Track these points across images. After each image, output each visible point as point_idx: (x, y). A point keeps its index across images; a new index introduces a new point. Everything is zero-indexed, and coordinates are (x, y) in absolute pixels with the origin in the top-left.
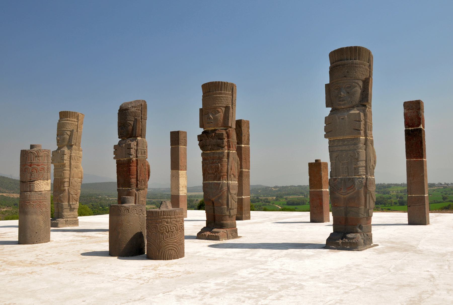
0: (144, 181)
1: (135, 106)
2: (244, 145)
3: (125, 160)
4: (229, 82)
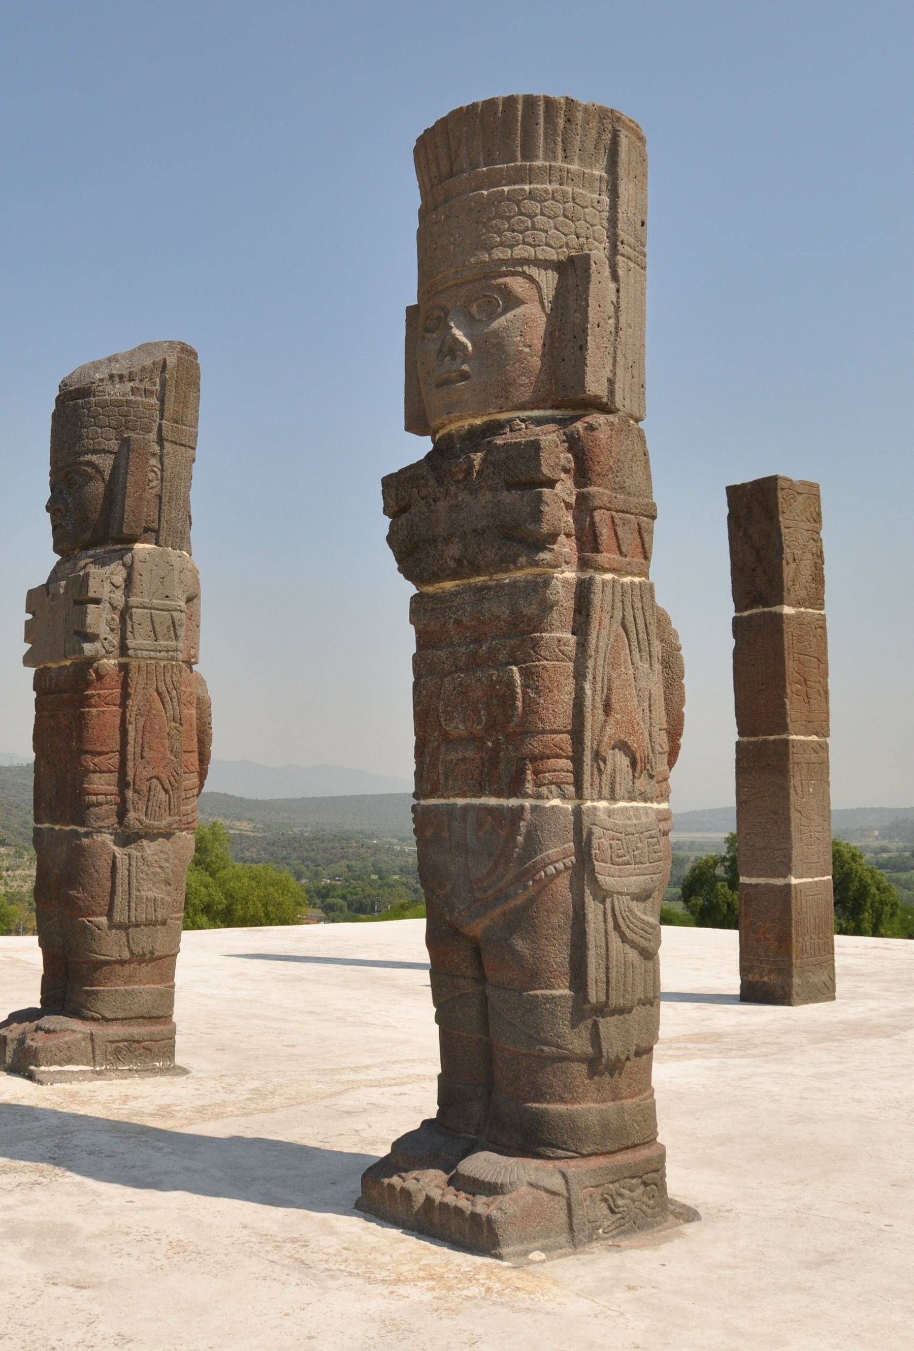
0: (166, 791)
1: (125, 373)
2: (793, 606)
3: (65, 666)
4: (583, 99)
